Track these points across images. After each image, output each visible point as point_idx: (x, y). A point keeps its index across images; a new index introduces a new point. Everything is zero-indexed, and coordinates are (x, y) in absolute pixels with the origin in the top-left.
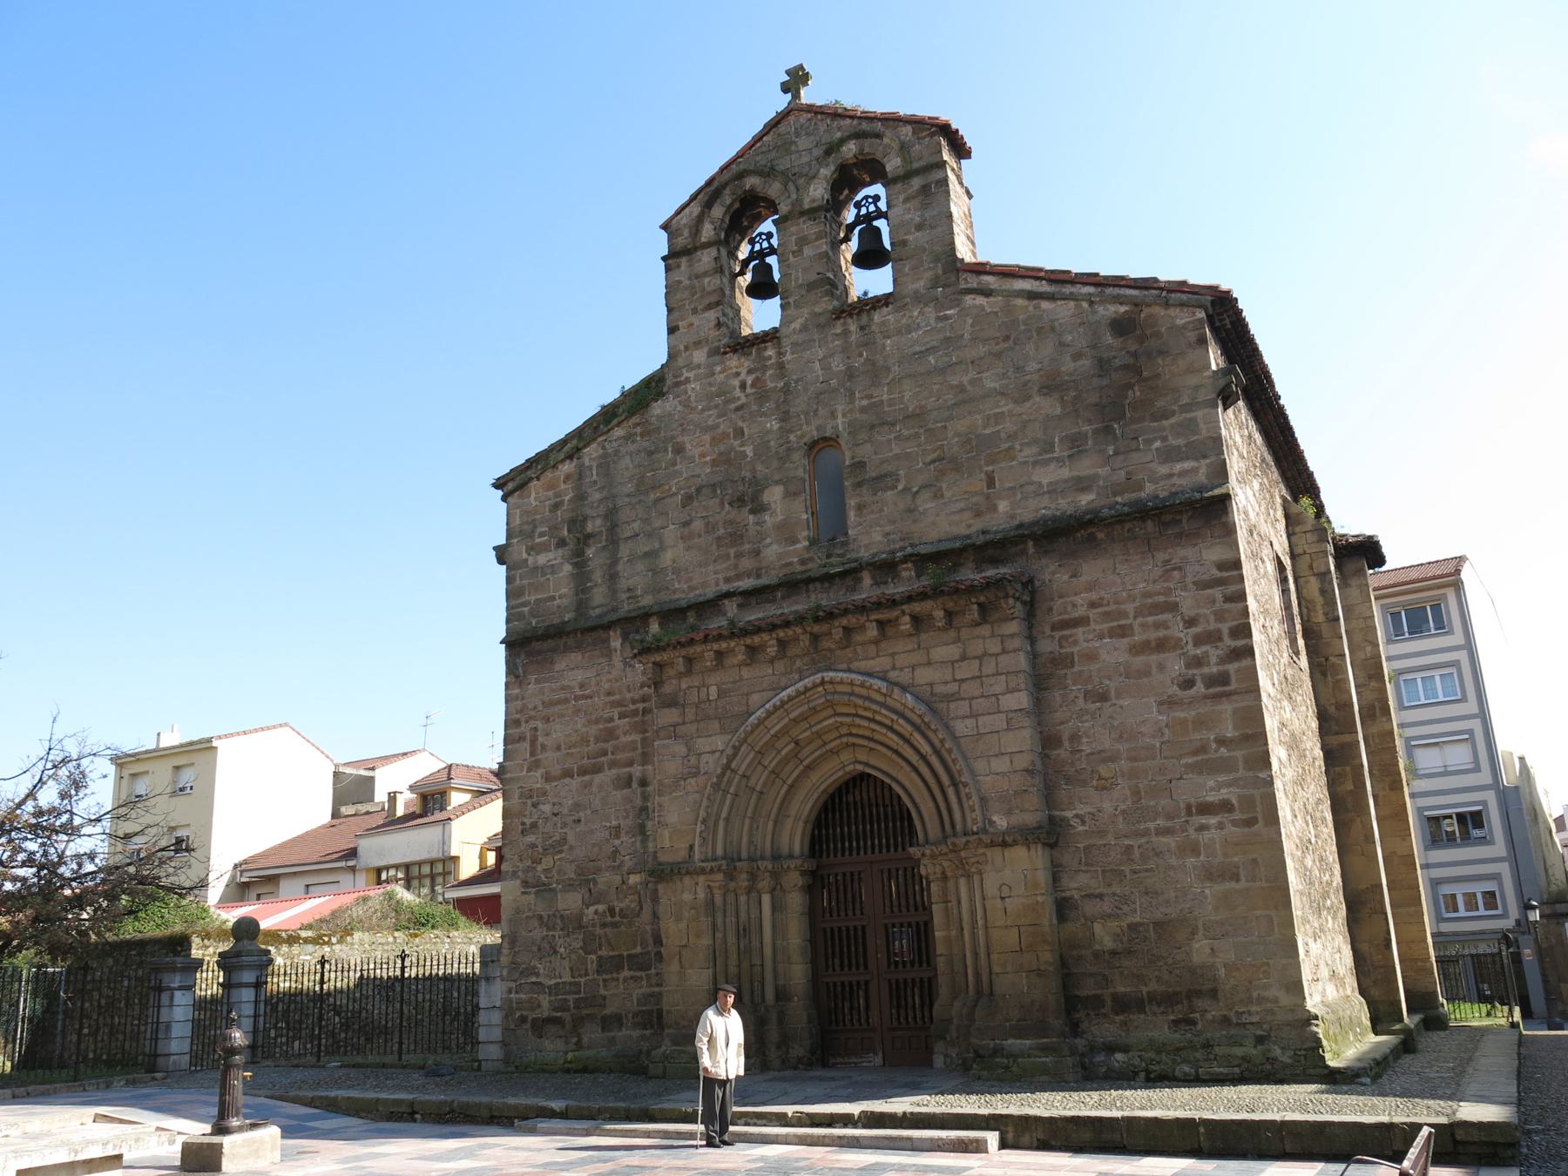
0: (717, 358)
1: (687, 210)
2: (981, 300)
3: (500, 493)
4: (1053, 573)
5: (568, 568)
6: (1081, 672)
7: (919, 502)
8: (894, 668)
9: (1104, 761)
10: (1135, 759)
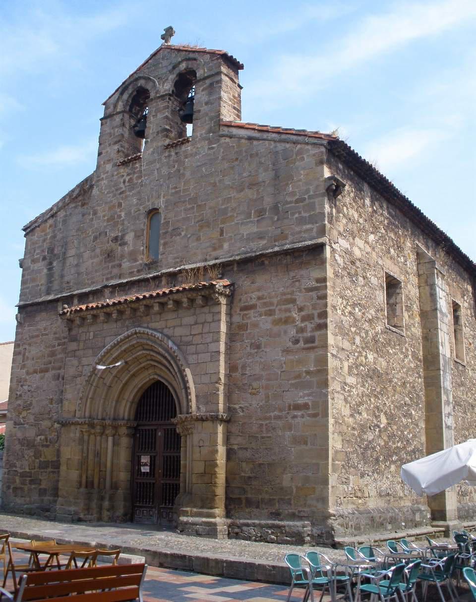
0: (116, 168)
2: (228, 140)
3: (24, 233)
4: (243, 281)
5: (45, 271)
6: (250, 333)
7: (190, 241)
8: (166, 327)
9: (256, 380)
10: (269, 380)
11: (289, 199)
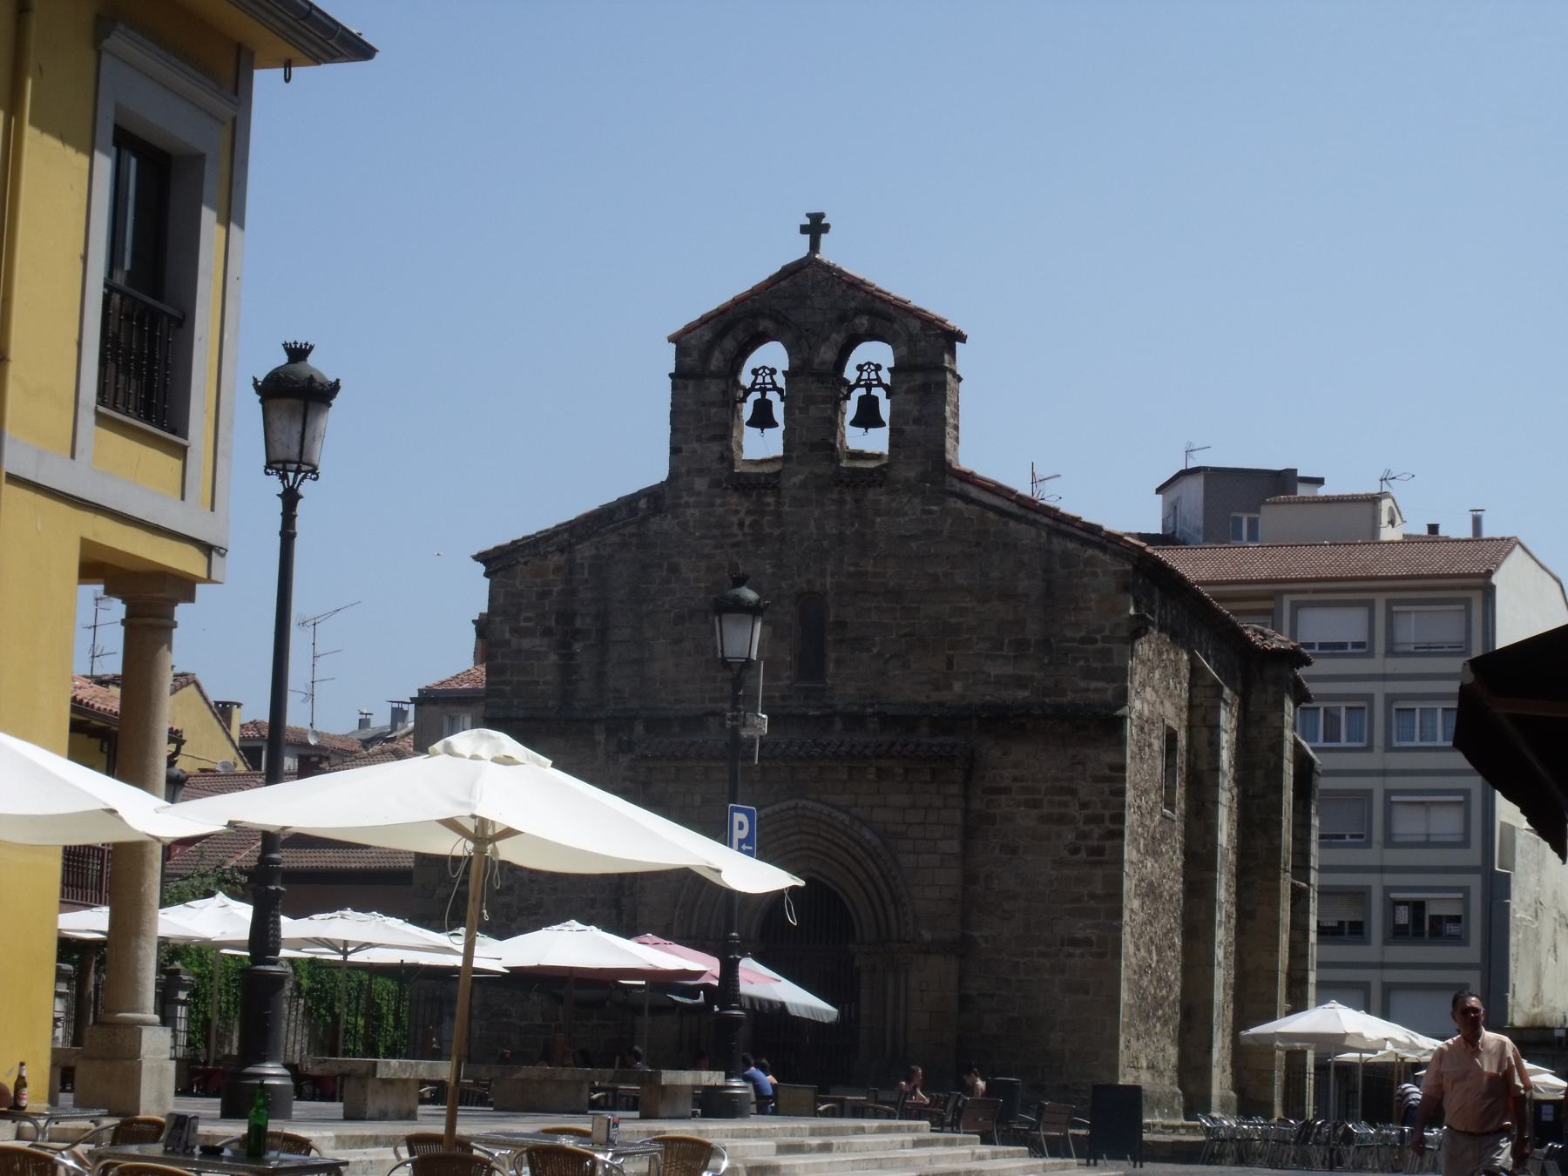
1: (698, 331)
2: (960, 504)
5: (553, 658)
11: (1068, 634)
